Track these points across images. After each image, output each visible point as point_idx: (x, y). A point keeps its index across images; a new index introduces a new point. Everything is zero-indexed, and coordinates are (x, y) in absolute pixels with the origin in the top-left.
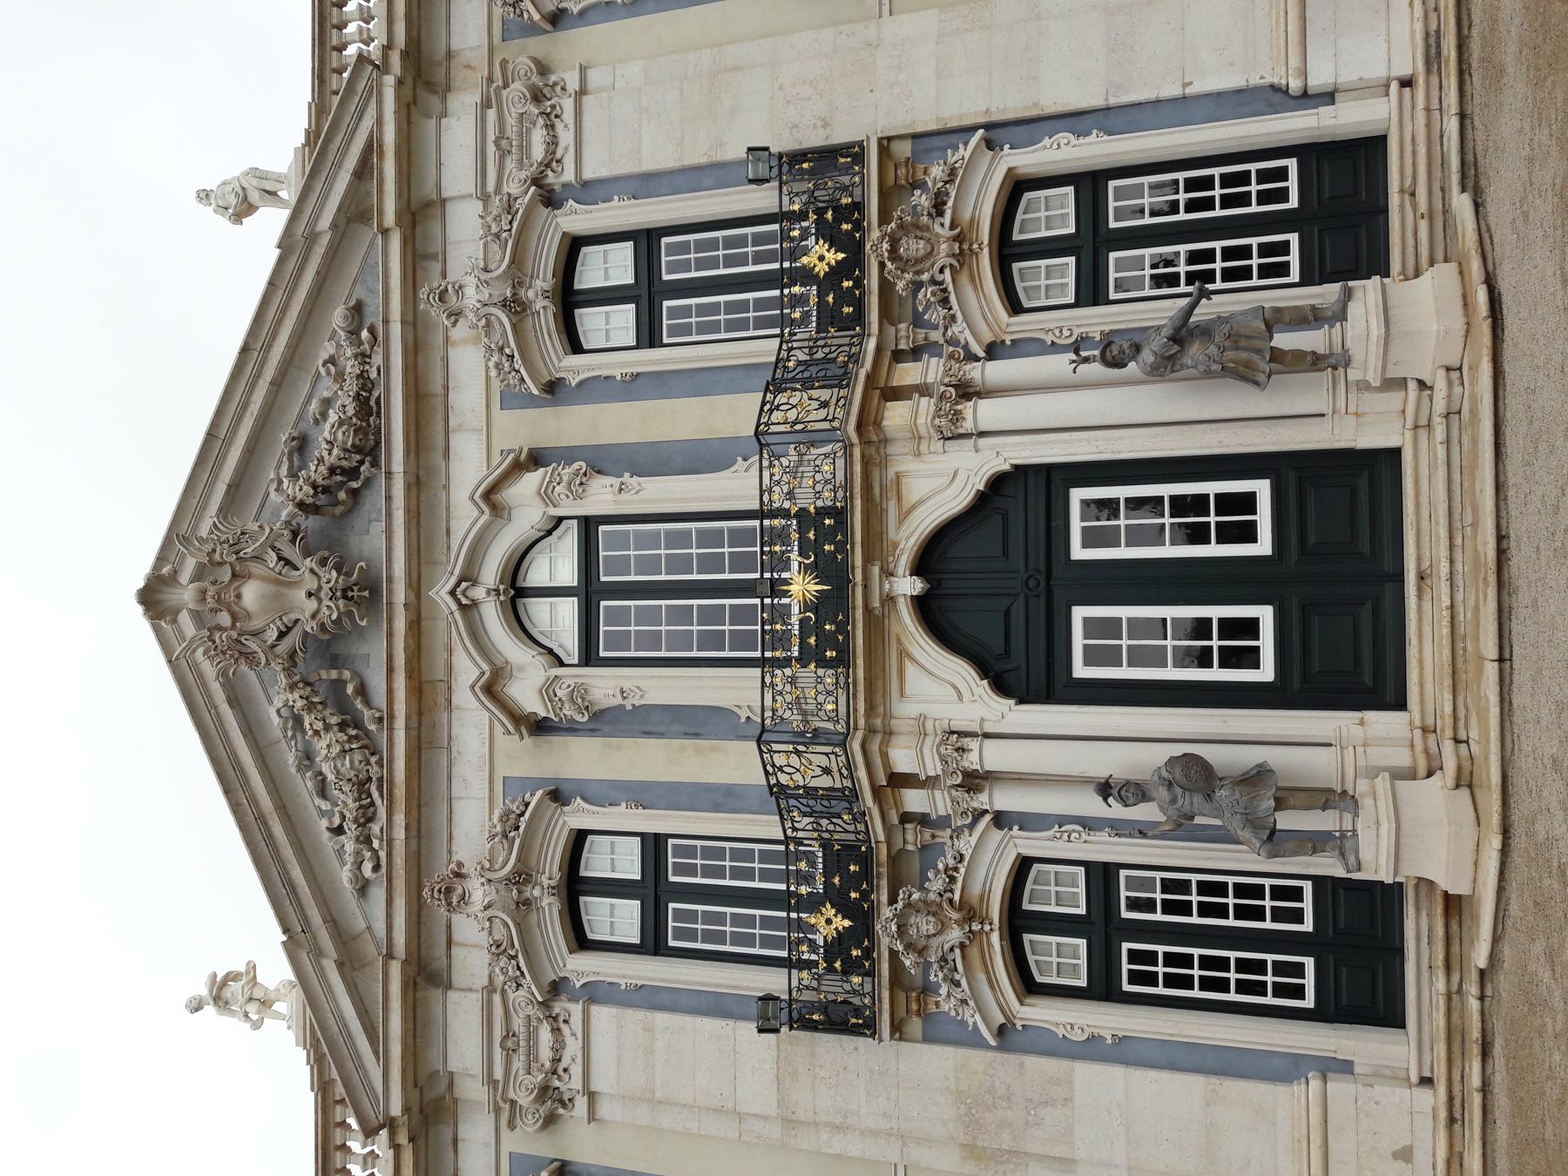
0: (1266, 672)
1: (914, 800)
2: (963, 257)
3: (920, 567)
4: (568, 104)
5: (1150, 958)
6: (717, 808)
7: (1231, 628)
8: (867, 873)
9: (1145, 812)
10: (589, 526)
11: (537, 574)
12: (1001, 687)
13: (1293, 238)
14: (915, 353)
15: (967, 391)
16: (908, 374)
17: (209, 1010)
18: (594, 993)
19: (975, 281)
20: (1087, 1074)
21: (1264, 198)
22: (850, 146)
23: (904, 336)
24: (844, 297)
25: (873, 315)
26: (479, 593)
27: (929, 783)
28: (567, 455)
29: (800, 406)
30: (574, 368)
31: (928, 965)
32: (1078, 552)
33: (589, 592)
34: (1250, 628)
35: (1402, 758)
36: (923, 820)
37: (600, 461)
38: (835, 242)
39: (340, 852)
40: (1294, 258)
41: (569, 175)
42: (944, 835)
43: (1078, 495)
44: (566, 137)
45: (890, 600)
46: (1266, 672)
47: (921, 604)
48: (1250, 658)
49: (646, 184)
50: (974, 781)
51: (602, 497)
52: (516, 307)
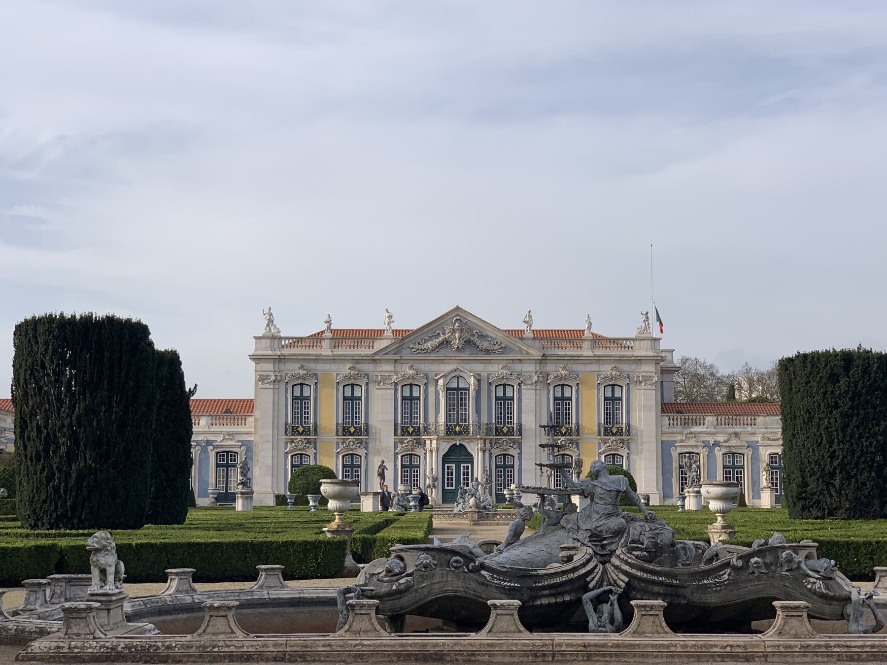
0: (446, 488)
1: (428, 442)
4: (534, 387)
5: (407, 472)
7: (452, 484)
8: (417, 435)
10: (468, 389)
11: (461, 380)
14: (491, 443)
15: (484, 451)
16: (488, 442)
17: (387, 315)
18: (396, 390)
19: (500, 451)
20: (393, 464)
23: (493, 442)
24: (499, 433)
25: (496, 437)
26: (458, 373)
27: (431, 446)
28: (479, 386)
29: (484, 427)
30: (493, 388)
32: (462, 465)
33: (458, 389)
34: (452, 486)
35: (437, 502)
36: (425, 443)
37: (478, 392)
38: (507, 432)
39: (415, 344)
40: (500, 492)
41: (523, 387)
42: (423, 445)
43: (470, 465)
44: (529, 387)
45: (456, 441)
46: (446, 488)
49: (520, 400)
51: (472, 393)
52: (503, 378)
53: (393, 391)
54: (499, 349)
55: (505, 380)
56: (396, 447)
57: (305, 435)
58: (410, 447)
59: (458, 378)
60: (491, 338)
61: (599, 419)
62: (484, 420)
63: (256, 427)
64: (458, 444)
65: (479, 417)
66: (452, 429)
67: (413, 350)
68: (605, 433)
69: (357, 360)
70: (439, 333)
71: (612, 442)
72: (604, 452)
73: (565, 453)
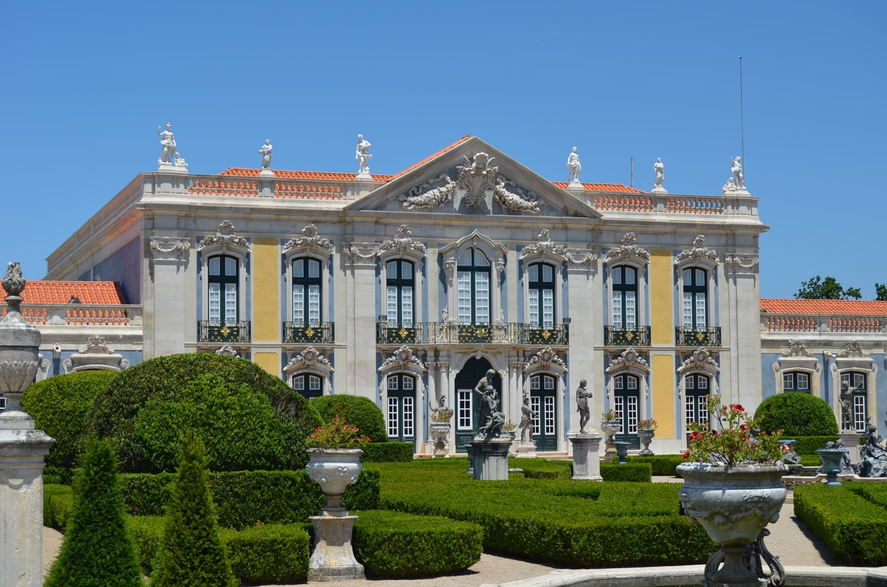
2: (543, 367)
3: (482, 358)
6: (423, 302)
9: (435, 404)
12: (458, 375)
13: (539, 434)
14: (524, 356)
15: (517, 368)
20: (374, 389)
21: (548, 428)
22: (568, 340)
31: (395, 356)
33: (473, 269)
34: (468, 424)
45: (476, 351)
46: (460, 428)
47: (473, 358)
48: (462, 424)
49: (565, 288)
50: (437, 369)
53: (374, 272)
54: (535, 207)
55: (543, 256)
56: (379, 364)
57: (232, 341)
58: (401, 363)
59: (473, 251)
60: (522, 188)
61: (677, 319)
62: (513, 318)
63: (145, 327)
64: (478, 358)
65: (506, 316)
66: (472, 333)
67: (405, 204)
68: (210, 336)
70: (444, 179)
71: (698, 354)
72: (685, 371)
73: (631, 372)
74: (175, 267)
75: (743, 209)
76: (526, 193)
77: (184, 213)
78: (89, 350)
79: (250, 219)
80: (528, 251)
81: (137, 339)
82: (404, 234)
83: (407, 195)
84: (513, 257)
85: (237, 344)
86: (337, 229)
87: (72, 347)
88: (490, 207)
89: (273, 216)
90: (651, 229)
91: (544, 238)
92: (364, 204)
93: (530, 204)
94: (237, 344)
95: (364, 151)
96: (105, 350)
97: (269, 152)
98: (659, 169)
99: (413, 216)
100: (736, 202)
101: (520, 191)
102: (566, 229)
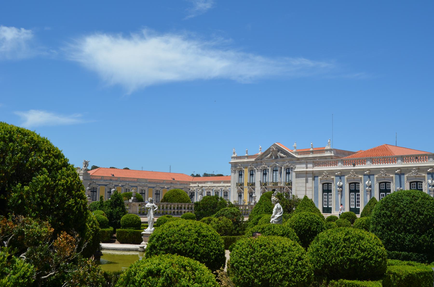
69: (252, 162)
74: (234, 173)
75: (329, 152)
76: (284, 154)
77: (235, 163)
78: (225, 188)
79: (244, 164)
80: (284, 166)
81: (230, 186)
82: (264, 164)
83: (265, 156)
84: (283, 167)
85: (241, 187)
86: (256, 164)
87: (223, 188)
88: (279, 158)
89: (247, 163)
90: (309, 159)
91: (287, 163)
92: (258, 159)
93: (285, 156)
94: (241, 187)
95: (260, 148)
96: (227, 188)
97: (247, 151)
98: (312, 145)
99: (265, 161)
100: (327, 150)
101: (284, 153)
102: (292, 160)
